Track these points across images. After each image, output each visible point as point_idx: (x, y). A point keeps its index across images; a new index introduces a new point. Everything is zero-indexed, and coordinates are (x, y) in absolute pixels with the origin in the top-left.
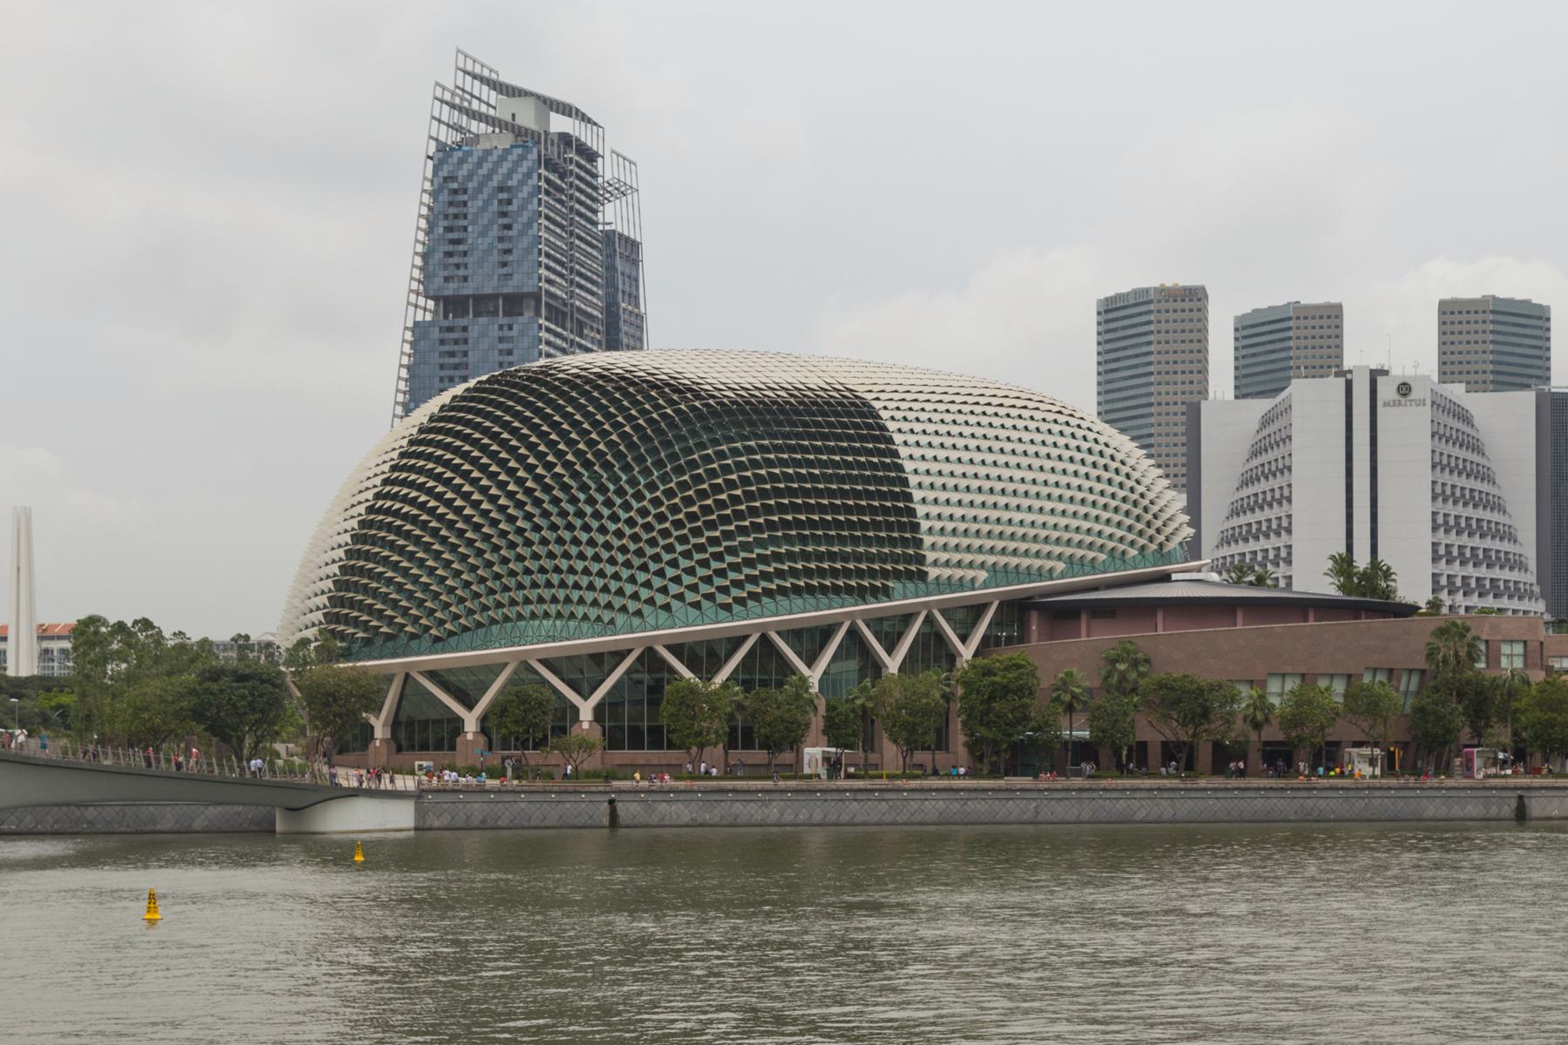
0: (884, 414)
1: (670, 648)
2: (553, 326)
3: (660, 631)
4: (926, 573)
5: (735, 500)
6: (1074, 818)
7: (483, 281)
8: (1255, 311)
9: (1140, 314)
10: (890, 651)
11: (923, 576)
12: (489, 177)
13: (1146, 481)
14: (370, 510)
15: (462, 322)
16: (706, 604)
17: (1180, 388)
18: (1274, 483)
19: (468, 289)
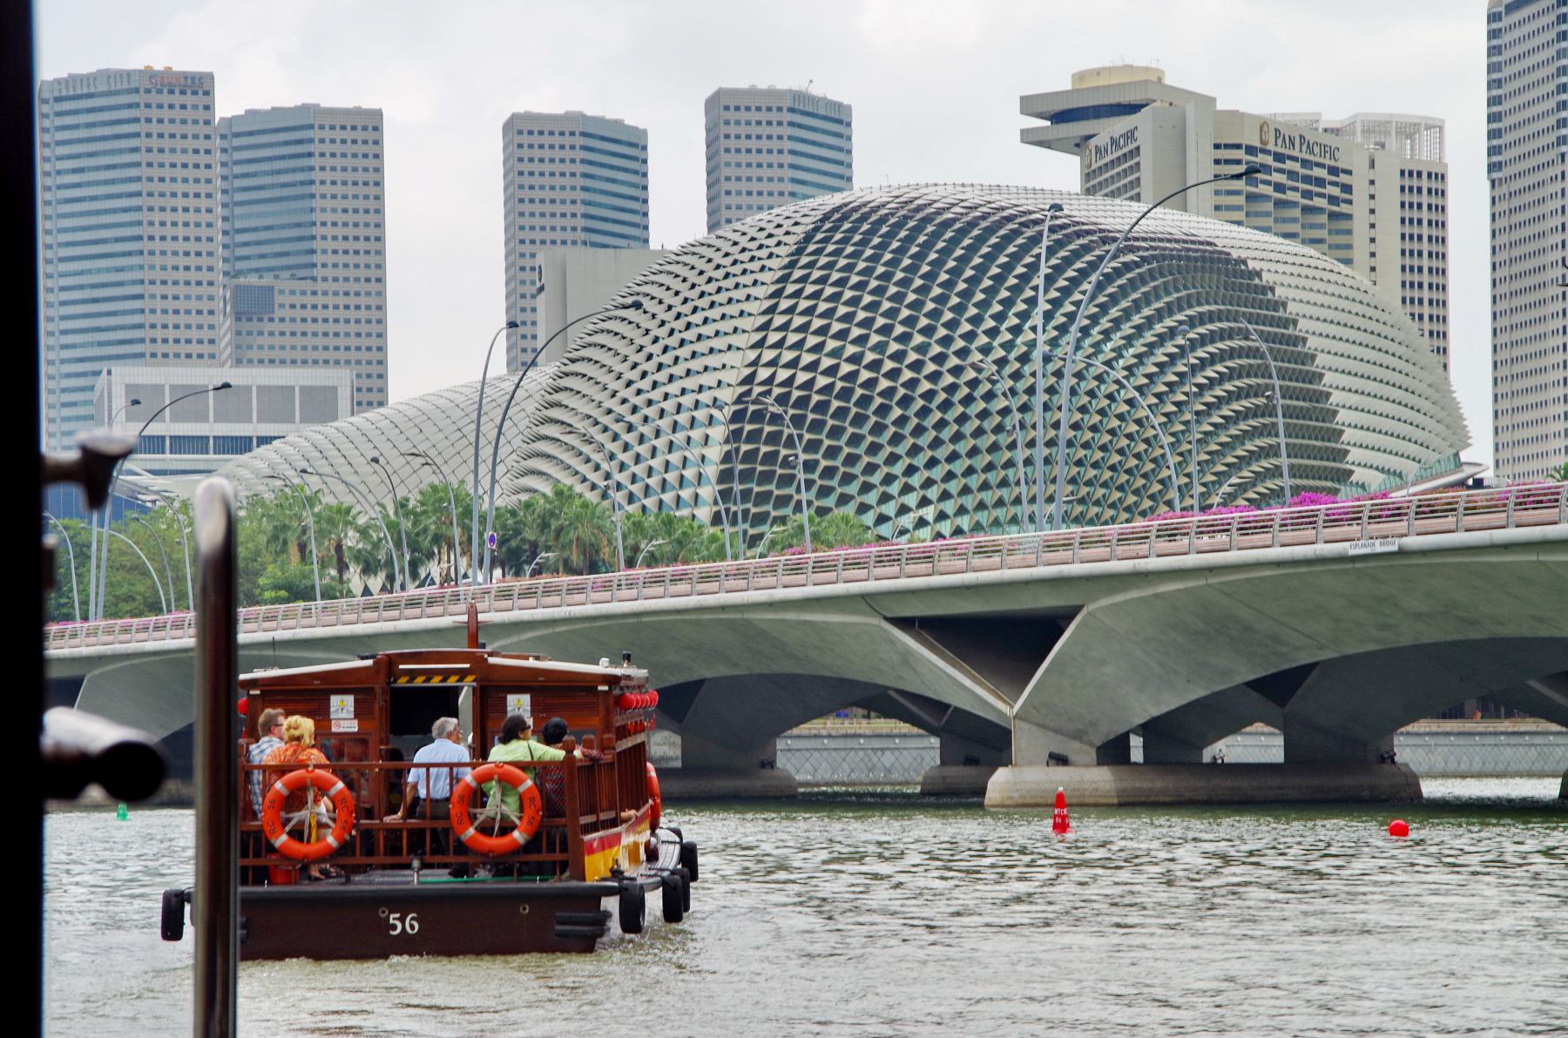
8: (251, 113)
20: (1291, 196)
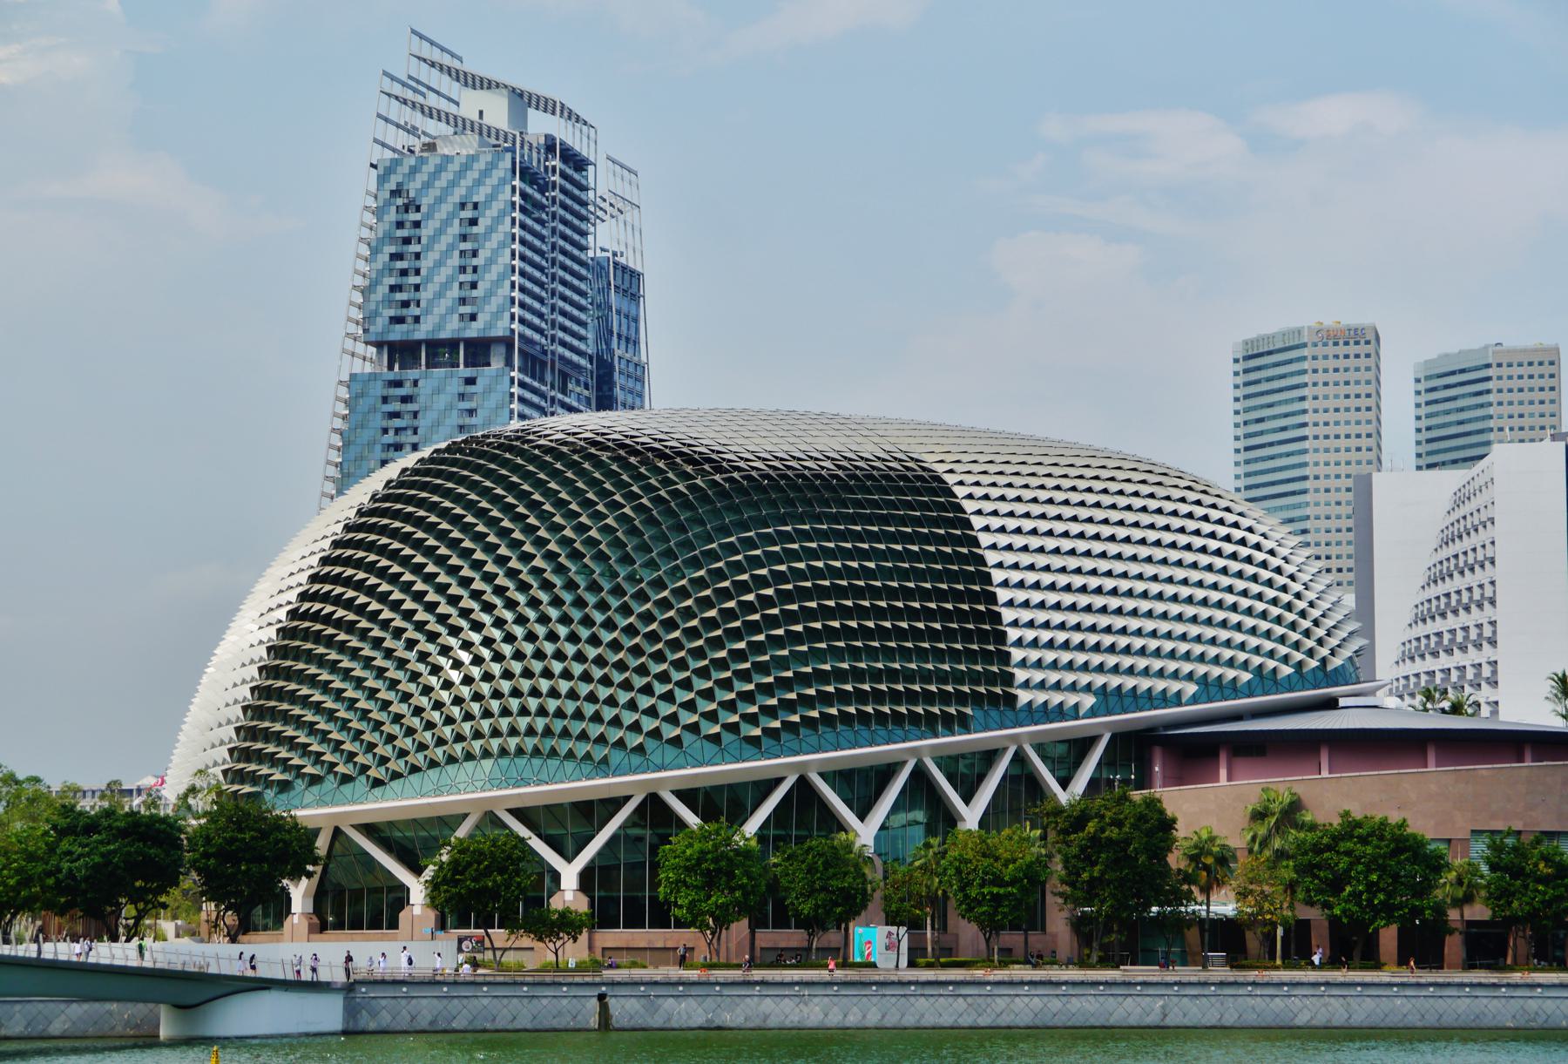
0: (960, 492)
1: (679, 794)
2: (528, 380)
3: (669, 776)
4: (1015, 697)
5: (766, 602)
6: (1213, 1022)
7: (438, 319)
9: (1290, 362)
10: (967, 800)
11: (1011, 699)
12: (447, 191)
13: (1305, 577)
14: (293, 614)
15: (412, 374)
16: (727, 737)
17: (1343, 456)
18: (1470, 579)
19: (422, 332)
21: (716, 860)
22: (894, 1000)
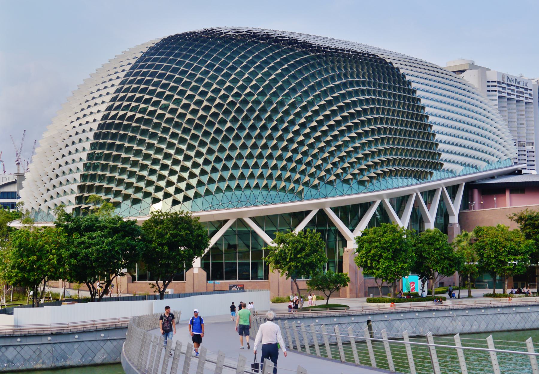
20: (512, 97)
21: (399, 244)
22: (491, 317)
